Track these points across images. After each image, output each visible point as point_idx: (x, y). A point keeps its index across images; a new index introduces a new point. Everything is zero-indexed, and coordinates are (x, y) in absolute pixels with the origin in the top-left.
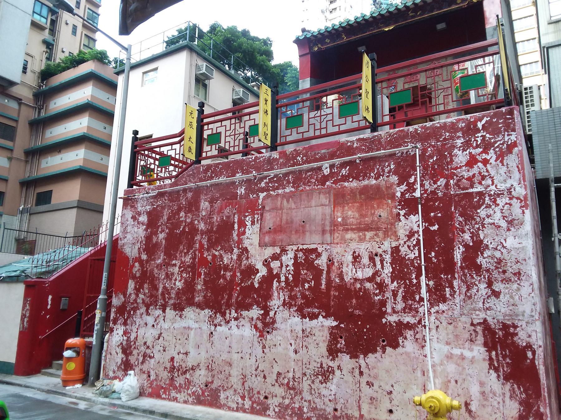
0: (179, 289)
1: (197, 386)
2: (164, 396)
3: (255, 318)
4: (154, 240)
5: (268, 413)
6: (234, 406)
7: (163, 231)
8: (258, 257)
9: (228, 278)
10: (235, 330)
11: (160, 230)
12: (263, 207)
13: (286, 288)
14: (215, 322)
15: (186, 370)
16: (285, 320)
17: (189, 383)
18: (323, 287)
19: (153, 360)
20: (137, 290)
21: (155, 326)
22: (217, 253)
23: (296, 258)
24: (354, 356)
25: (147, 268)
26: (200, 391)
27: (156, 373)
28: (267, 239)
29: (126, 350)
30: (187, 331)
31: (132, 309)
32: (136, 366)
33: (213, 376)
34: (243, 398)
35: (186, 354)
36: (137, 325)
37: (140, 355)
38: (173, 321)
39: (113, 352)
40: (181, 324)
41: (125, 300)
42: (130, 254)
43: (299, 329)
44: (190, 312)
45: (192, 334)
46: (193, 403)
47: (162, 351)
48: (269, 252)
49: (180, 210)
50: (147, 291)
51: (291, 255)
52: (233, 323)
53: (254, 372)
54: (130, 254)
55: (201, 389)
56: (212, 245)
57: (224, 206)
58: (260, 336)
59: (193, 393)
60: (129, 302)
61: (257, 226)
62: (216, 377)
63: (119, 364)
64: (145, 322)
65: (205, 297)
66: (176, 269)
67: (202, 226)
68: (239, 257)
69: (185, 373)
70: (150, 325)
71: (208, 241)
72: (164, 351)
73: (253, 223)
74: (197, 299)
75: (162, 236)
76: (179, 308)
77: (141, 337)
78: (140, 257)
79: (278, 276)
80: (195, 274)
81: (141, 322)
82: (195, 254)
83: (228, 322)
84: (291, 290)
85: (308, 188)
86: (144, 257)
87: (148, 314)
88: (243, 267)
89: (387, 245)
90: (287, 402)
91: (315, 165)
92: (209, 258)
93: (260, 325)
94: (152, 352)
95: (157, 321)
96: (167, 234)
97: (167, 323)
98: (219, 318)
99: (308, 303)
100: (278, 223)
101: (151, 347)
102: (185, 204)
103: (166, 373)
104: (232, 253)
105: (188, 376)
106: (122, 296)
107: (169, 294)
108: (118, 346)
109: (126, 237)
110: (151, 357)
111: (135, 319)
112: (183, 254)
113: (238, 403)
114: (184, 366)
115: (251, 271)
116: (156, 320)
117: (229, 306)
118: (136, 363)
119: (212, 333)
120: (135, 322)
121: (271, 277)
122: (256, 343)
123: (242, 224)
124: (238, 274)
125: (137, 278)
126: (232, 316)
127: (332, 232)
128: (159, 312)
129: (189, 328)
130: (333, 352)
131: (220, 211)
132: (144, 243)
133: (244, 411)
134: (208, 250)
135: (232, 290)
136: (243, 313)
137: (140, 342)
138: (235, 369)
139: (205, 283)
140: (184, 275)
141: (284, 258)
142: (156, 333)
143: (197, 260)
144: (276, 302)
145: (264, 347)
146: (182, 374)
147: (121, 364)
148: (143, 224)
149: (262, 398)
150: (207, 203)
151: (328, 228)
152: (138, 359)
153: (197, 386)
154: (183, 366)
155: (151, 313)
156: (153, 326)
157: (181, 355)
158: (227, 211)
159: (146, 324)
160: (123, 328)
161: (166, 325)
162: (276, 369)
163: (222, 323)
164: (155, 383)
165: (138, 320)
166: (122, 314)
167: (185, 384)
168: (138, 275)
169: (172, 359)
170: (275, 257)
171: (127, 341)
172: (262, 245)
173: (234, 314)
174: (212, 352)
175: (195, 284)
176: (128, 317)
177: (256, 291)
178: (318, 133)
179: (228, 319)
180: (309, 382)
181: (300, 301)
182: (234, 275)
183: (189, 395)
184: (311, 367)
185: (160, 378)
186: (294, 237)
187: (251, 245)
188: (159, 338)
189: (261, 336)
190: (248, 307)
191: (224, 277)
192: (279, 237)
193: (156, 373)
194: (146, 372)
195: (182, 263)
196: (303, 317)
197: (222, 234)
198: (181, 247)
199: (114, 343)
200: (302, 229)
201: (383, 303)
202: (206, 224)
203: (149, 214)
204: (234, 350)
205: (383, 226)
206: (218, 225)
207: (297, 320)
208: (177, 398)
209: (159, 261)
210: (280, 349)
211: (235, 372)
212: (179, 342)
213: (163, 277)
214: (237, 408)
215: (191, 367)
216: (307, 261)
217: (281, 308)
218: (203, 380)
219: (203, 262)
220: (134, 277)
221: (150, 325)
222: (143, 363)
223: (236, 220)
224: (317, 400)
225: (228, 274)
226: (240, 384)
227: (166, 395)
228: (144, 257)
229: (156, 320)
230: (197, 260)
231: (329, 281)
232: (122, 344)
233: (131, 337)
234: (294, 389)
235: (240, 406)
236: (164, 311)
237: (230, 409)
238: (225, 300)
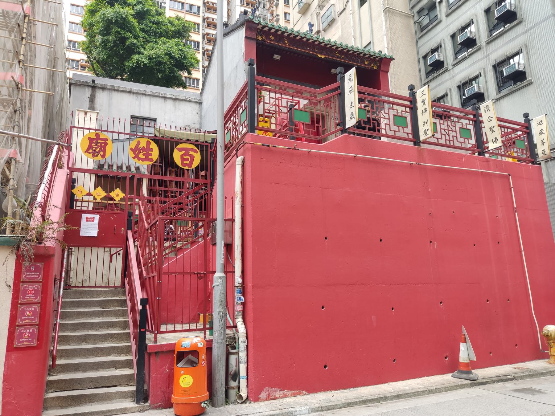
178: (448, 143)
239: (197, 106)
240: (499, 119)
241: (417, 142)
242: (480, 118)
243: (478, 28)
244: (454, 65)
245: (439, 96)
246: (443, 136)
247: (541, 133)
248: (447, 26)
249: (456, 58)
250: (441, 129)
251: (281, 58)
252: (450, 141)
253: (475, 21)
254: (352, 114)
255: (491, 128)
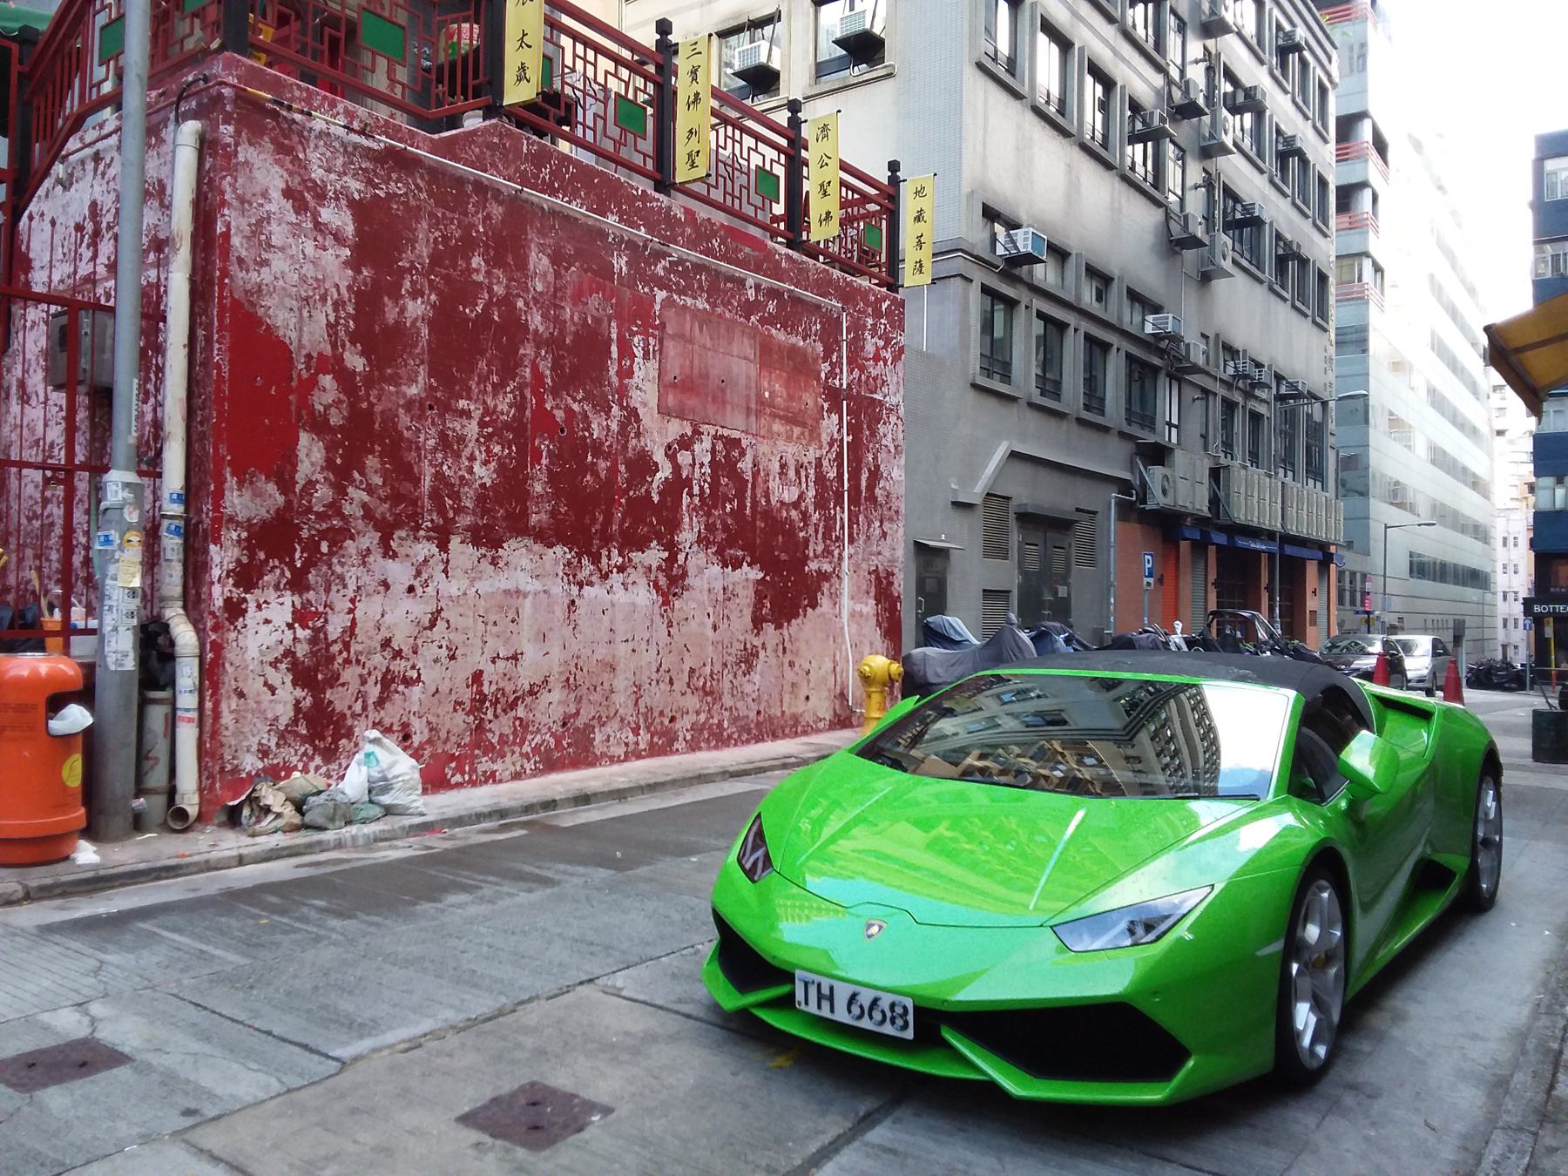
0: (483, 486)
1: (544, 730)
2: (458, 778)
3: (654, 567)
4: (391, 314)
5: (676, 745)
6: (620, 751)
7: (415, 294)
8: (657, 435)
9: (603, 474)
10: (620, 595)
11: (407, 284)
12: (663, 325)
13: (701, 508)
14: (580, 576)
15: (517, 698)
16: (701, 571)
17: (524, 726)
18: (748, 511)
19: (416, 690)
20: (341, 474)
21: (419, 591)
22: (576, 407)
23: (713, 451)
24: (779, 626)
25: (372, 405)
26: (552, 740)
27: (428, 723)
28: (671, 400)
29: (312, 670)
30: (514, 601)
31: (323, 535)
32: (355, 716)
33: (579, 700)
34: (636, 732)
35: (515, 658)
36: (352, 586)
37: (371, 681)
38: (473, 575)
39: (254, 687)
40: (493, 583)
41: (289, 503)
42: (294, 335)
43: (718, 586)
44: (517, 552)
45: (527, 606)
46: (537, 773)
47: (445, 661)
48: (676, 428)
49: (468, 244)
50: (379, 481)
51: (707, 444)
52: (616, 578)
53: (654, 676)
54: (294, 335)
55: (553, 735)
56: (566, 382)
57: (586, 286)
58: (664, 604)
59: (536, 750)
60: (309, 510)
61: (653, 365)
62: (584, 701)
63: (284, 721)
64: (379, 577)
65: (554, 513)
66: (472, 429)
67: (536, 321)
68: (623, 426)
69: (513, 706)
70: (399, 588)
71: (553, 369)
72: (452, 658)
73: (646, 356)
74: (534, 518)
75: (416, 309)
76: (487, 539)
77: (371, 624)
78: (340, 359)
79: (688, 482)
80: (528, 454)
81: (366, 579)
82: (523, 396)
83: (605, 577)
84: (708, 514)
85: (728, 315)
86: (356, 361)
87: (389, 553)
88: (630, 454)
89: (812, 454)
90: (703, 717)
91: (739, 272)
92: (559, 415)
93: (663, 581)
94: (413, 667)
95: (425, 576)
96: (433, 306)
97: (454, 582)
98: (587, 567)
99: (730, 542)
100: (687, 371)
101: (406, 651)
102: (485, 233)
103: (460, 717)
104: (608, 417)
105: (521, 711)
106: (271, 488)
107: (456, 496)
108: (274, 664)
109: (265, 263)
110: (408, 682)
111: (338, 569)
112: (489, 388)
113: (627, 745)
114: (509, 688)
115: (643, 466)
116: (418, 573)
117: (606, 540)
118: (358, 708)
119: (573, 602)
120: (342, 578)
121: (678, 484)
122: (657, 618)
123: (626, 351)
124: (622, 468)
125: (332, 430)
126: (613, 562)
127: (758, 414)
128: (425, 549)
129: (518, 591)
130: (758, 622)
131: (578, 298)
132: (350, 309)
133: (639, 757)
134: (555, 393)
135: (611, 502)
136: (633, 555)
137: (366, 639)
138: (621, 677)
139: (553, 479)
140: (497, 449)
141: (696, 447)
142: (421, 609)
143: (528, 413)
144: (686, 537)
145: (670, 625)
146: (504, 711)
147: (295, 721)
148: (338, 238)
149: (666, 722)
150: (545, 260)
151: (753, 406)
152: (361, 695)
153: (544, 730)
154: (507, 690)
155: (402, 551)
156: (411, 589)
157: (501, 664)
158: (594, 301)
159: (386, 585)
160: (288, 598)
161: (452, 587)
162: (689, 663)
163: (594, 579)
164: (427, 753)
165: (352, 574)
166: (285, 554)
167: (515, 733)
168: (335, 419)
169: (477, 677)
170: (685, 443)
171: (313, 641)
172: (664, 411)
173: (617, 559)
174: (574, 647)
175: (527, 477)
176: (309, 564)
177: (656, 509)
179: (605, 569)
180: (731, 677)
181: (720, 536)
182: (613, 470)
183: (527, 756)
184: (733, 651)
185: (443, 735)
186: (711, 409)
187: (645, 404)
188: (433, 624)
189: (666, 603)
190: (642, 546)
191: (592, 468)
192: (692, 402)
193: (428, 723)
194: (395, 728)
195: (487, 411)
196: (725, 565)
197: (584, 362)
198: (482, 365)
199: (253, 652)
200: (719, 398)
201: (806, 541)
202: (545, 317)
203: (360, 210)
204: (620, 637)
205: (809, 422)
206: (576, 333)
207: (717, 569)
208: (493, 773)
209: (413, 391)
210: (693, 624)
211: (622, 683)
212: (495, 629)
213: (431, 442)
214: (626, 753)
215: (527, 688)
216: (726, 462)
217: (695, 547)
218: (557, 713)
219: (544, 420)
220: (319, 426)
221: (399, 588)
222: (380, 703)
223: (614, 336)
224: (739, 704)
225: (603, 465)
226: (631, 704)
227: (463, 775)
228: (356, 361)
229: (418, 573)
230: (528, 413)
231: (755, 503)
232: (289, 653)
233: (330, 628)
234: (711, 693)
235: (631, 747)
236: (443, 546)
237: (613, 760)
238: (598, 527)
240: (844, 167)
241: (664, 184)
242: (804, 153)
246: (721, 180)
247: (918, 219)
250: (718, 160)
252: (733, 197)
254: (523, 68)
255: (822, 185)
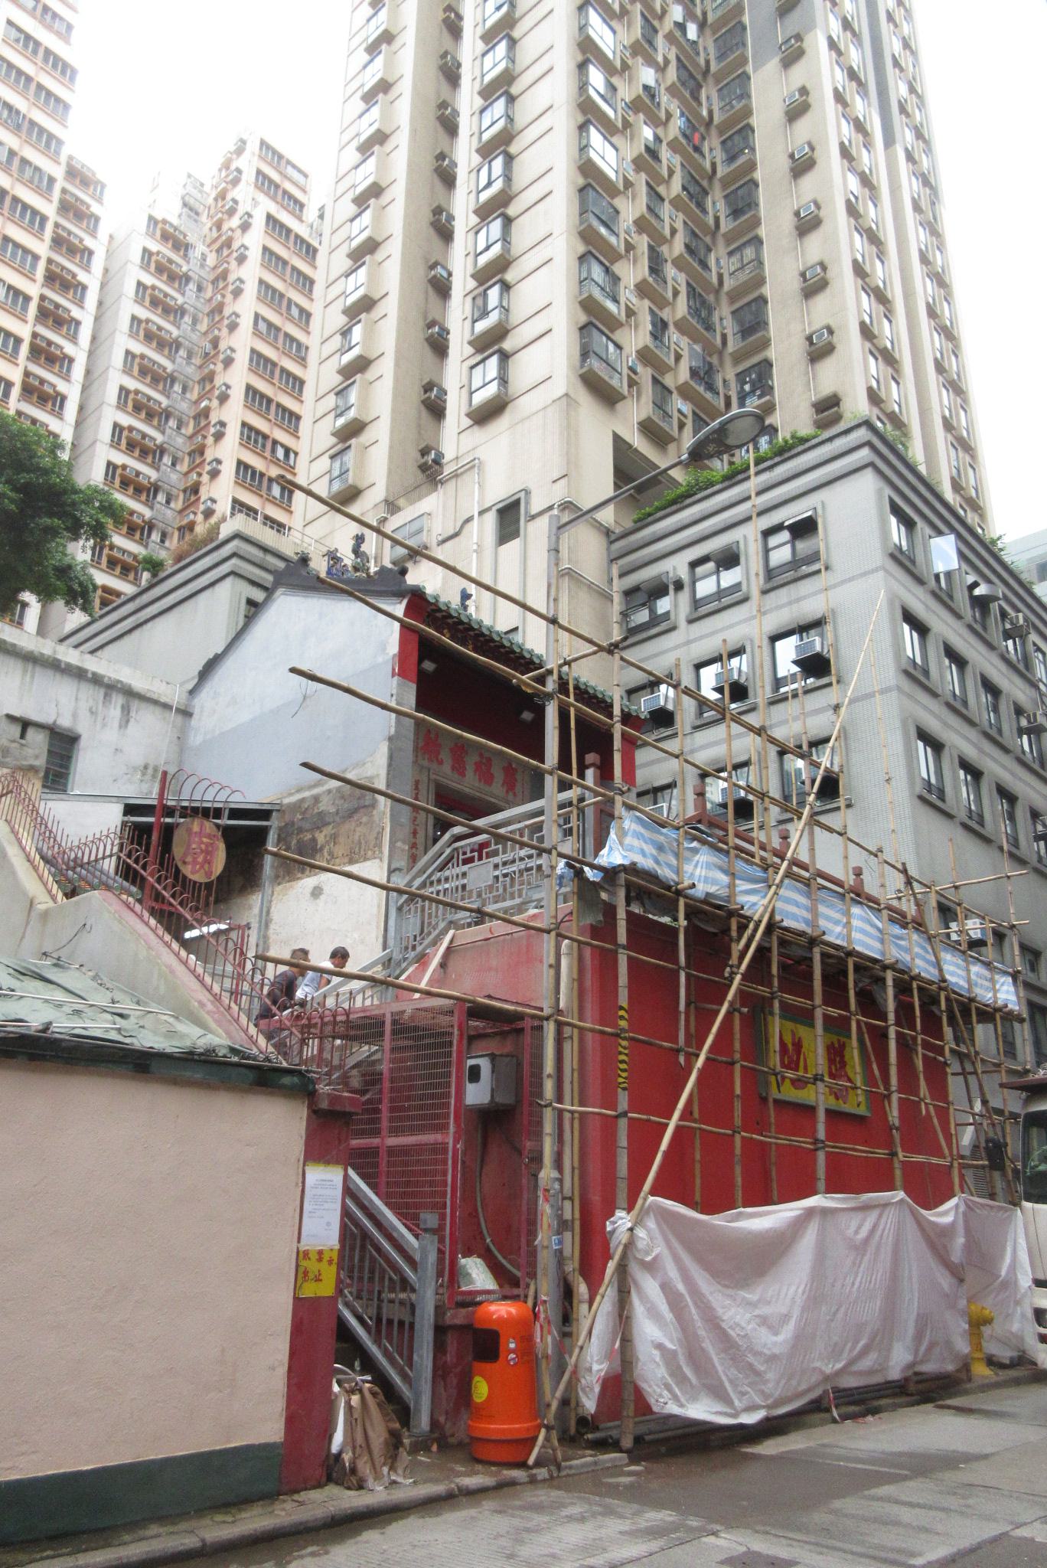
239: (180, 718)
243: (752, 664)
244: (697, 728)
245: (657, 784)
248: (689, 642)
249: (701, 714)
251: (436, 670)
253: (748, 649)
